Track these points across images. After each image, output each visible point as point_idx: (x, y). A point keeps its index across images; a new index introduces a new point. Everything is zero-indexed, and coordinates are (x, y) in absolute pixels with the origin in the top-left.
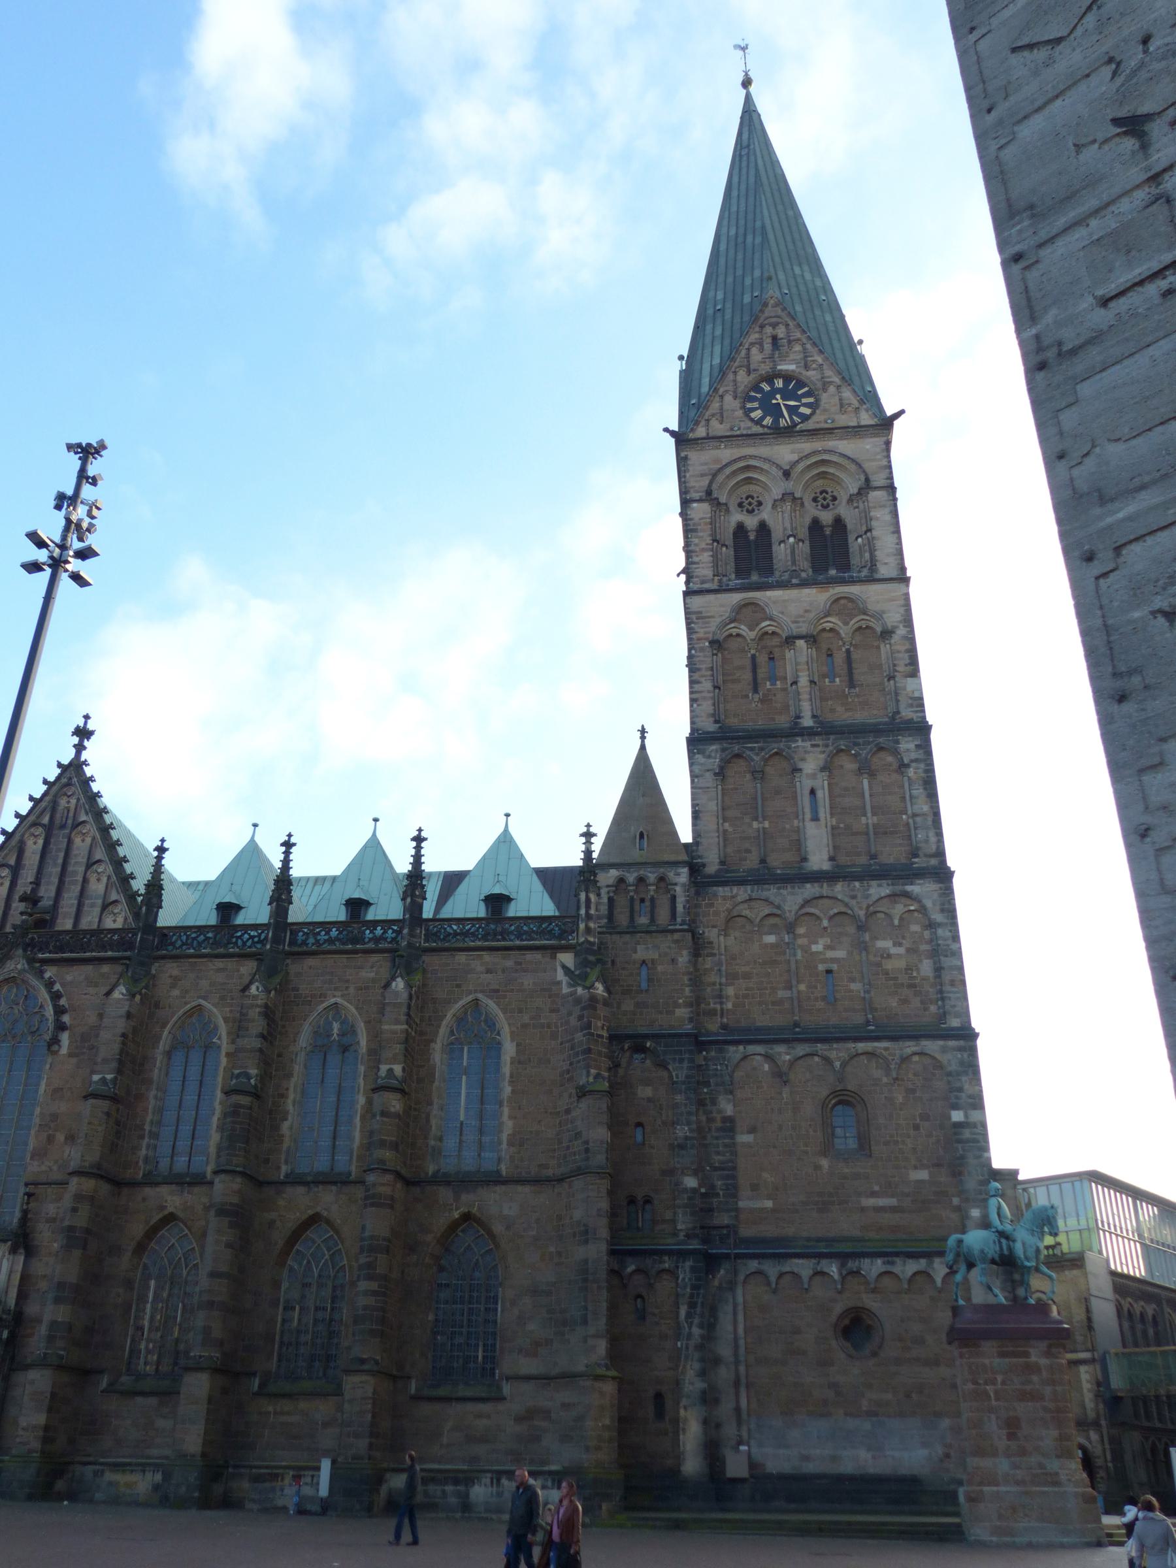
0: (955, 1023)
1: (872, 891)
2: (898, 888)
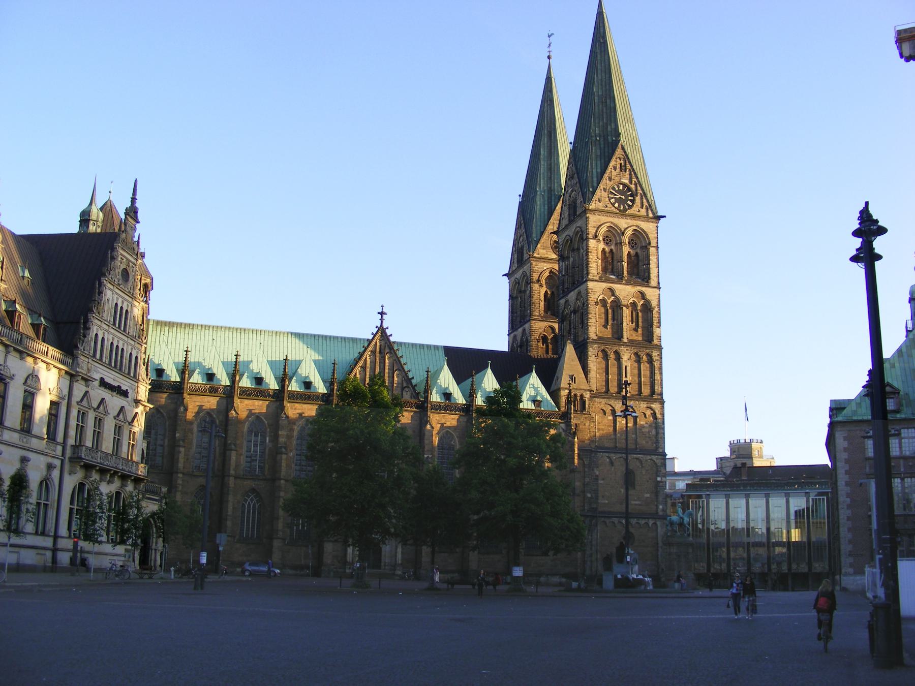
0: (661, 451)
1: (641, 405)
2: (649, 405)
